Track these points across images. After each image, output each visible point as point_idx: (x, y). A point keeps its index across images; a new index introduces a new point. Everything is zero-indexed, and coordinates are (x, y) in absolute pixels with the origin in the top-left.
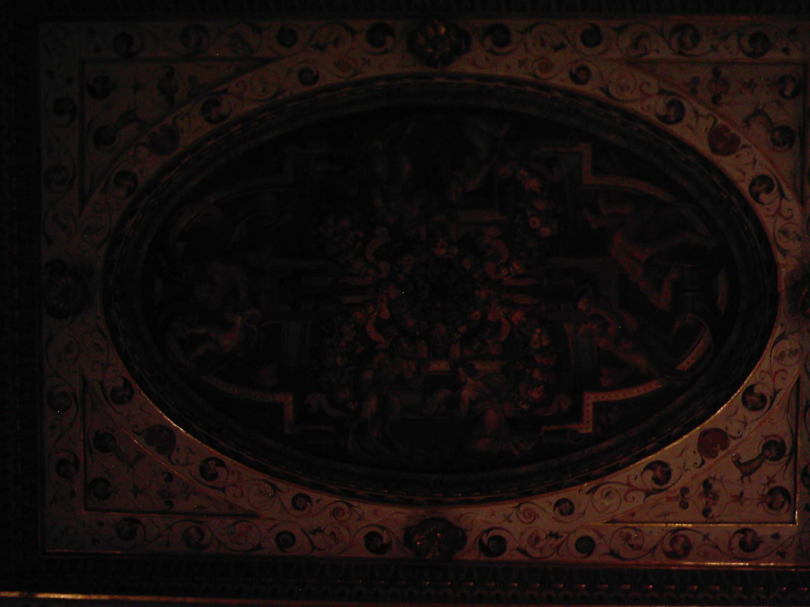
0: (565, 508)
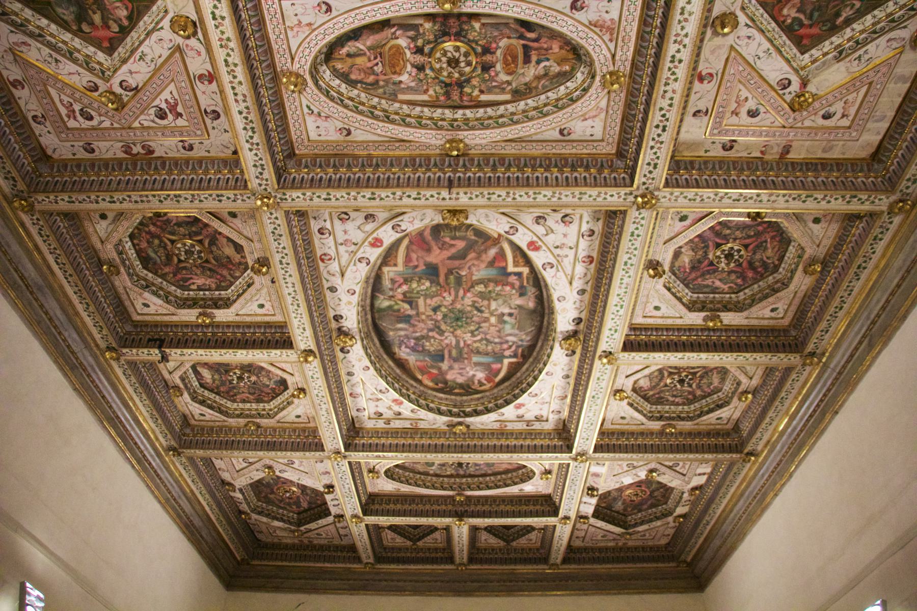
0: (561, 299)
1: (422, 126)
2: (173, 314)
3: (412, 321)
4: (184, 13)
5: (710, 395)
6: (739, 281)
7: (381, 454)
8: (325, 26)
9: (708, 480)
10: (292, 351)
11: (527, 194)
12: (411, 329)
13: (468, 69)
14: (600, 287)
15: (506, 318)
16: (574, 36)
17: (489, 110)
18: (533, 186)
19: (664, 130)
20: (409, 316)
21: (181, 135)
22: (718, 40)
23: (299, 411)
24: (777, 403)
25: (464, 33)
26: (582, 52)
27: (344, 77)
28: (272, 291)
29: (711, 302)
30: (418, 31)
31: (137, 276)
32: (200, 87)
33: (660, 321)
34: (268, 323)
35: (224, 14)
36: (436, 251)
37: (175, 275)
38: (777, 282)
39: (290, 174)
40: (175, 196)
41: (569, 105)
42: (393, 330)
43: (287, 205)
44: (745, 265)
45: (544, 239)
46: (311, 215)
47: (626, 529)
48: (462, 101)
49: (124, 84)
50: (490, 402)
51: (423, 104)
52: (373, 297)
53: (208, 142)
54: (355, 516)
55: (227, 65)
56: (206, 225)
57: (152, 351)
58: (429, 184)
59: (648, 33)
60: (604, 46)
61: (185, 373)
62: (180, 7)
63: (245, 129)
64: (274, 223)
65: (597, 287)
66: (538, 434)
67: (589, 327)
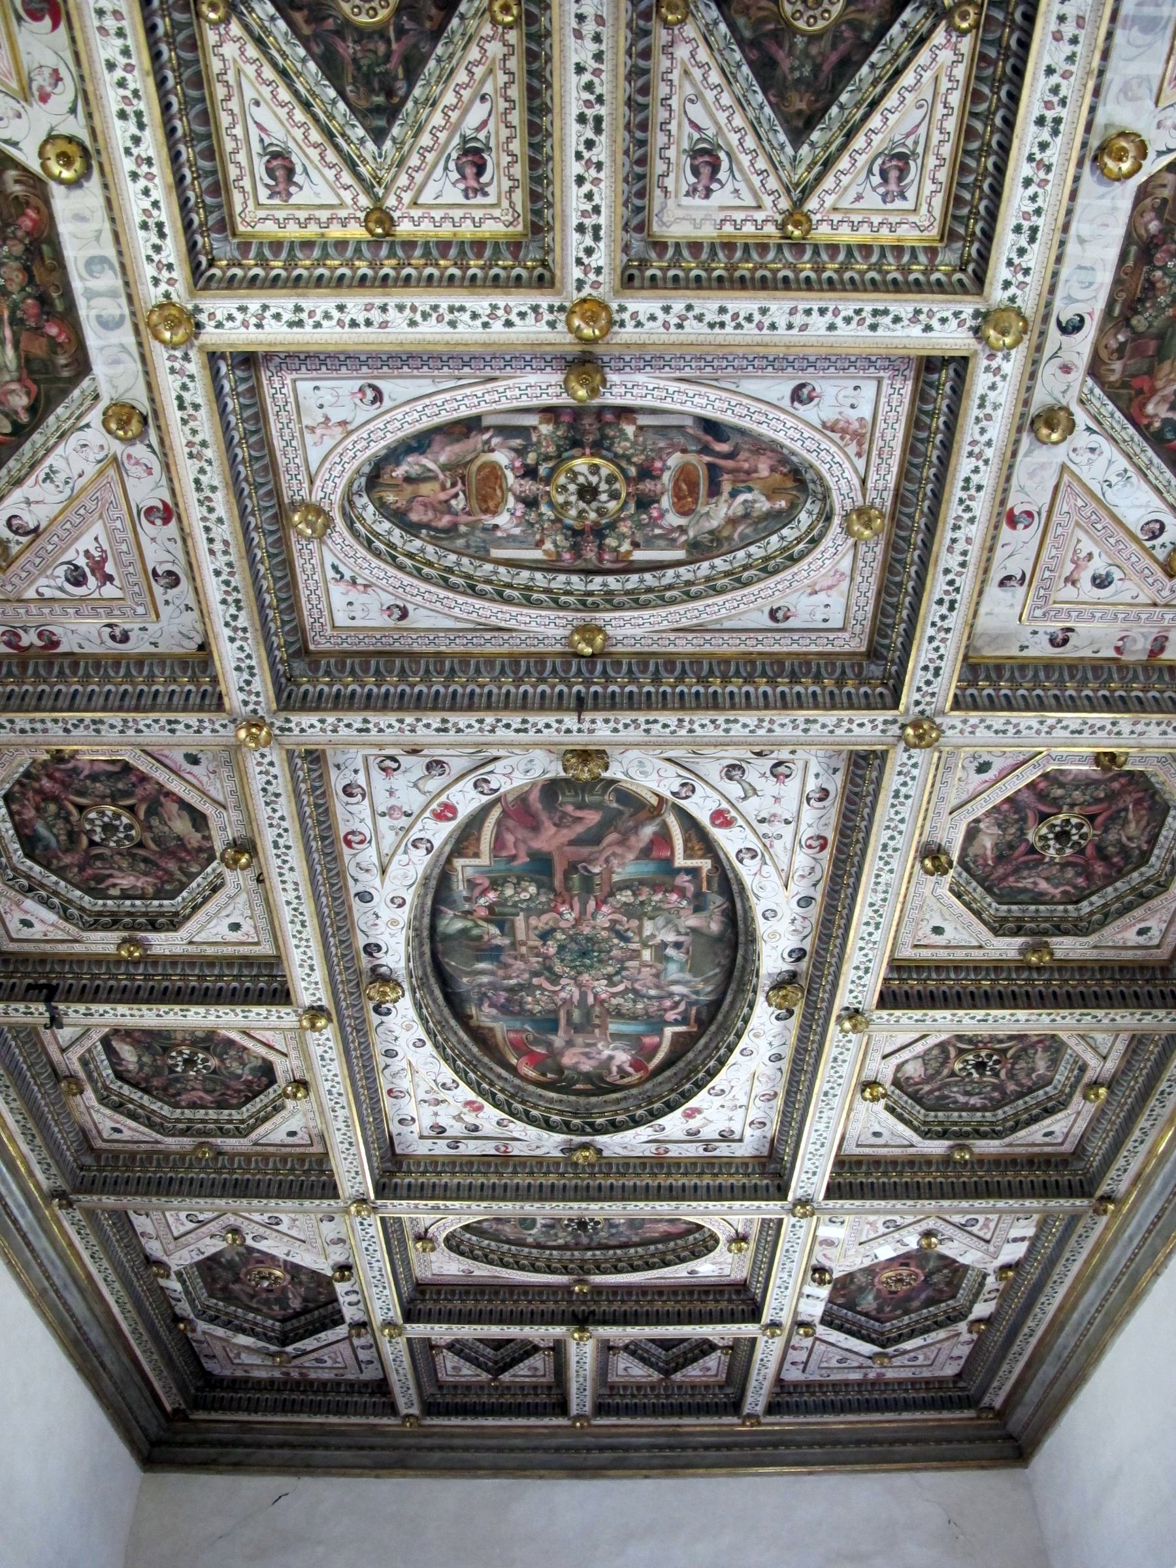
1: (529, 603)
2: (76, 941)
3: (505, 958)
4: (127, 398)
5: (1031, 1090)
6: (1080, 881)
7: (441, 1203)
8: (371, 426)
9: (1030, 1251)
10: (288, 1009)
11: (713, 722)
12: (501, 973)
13: (613, 505)
14: (838, 892)
15: (670, 951)
16: (796, 447)
17: (647, 576)
18: (724, 709)
19: (952, 608)
20: (499, 948)
21: (109, 614)
22: (1043, 455)
23: (294, 1124)
24: (1153, 1102)
25: (607, 443)
26: (808, 477)
27: (399, 517)
28: (257, 900)
29: (1033, 919)
30: (528, 438)
31: (14, 869)
32: (148, 530)
33: (943, 954)
34: (245, 957)
35: (199, 401)
36: (549, 829)
37: (82, 869)
38: (1148, 881)
39: (299, 685)
40: (94, 722)
41: (786, 568)
42: (468, 974)
43: (293, 740)
44: (1089, 851)
45: (742, 806)
46: (331, 761)
47: (883, 1346)
48: (601, 560)
49: (15, 522)
50: (639, 1107)
51: (534, 566)
52: (435, 914)
53: (157, 626)
54: (389, 1324)
55: (199, 489)
56: (144, 778)
57: (33, 1007)
58: (544, 704)
59: (922, 441)
60: (846, 465)
61: (89, 1051)
62: (121, 390)
63: (224, 602)
64: (267, 773)
65: (832, 893)
66: (727, 1164)
67: (819, 965)
